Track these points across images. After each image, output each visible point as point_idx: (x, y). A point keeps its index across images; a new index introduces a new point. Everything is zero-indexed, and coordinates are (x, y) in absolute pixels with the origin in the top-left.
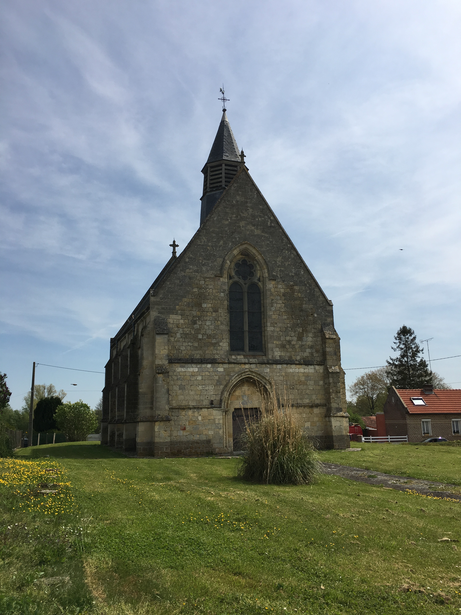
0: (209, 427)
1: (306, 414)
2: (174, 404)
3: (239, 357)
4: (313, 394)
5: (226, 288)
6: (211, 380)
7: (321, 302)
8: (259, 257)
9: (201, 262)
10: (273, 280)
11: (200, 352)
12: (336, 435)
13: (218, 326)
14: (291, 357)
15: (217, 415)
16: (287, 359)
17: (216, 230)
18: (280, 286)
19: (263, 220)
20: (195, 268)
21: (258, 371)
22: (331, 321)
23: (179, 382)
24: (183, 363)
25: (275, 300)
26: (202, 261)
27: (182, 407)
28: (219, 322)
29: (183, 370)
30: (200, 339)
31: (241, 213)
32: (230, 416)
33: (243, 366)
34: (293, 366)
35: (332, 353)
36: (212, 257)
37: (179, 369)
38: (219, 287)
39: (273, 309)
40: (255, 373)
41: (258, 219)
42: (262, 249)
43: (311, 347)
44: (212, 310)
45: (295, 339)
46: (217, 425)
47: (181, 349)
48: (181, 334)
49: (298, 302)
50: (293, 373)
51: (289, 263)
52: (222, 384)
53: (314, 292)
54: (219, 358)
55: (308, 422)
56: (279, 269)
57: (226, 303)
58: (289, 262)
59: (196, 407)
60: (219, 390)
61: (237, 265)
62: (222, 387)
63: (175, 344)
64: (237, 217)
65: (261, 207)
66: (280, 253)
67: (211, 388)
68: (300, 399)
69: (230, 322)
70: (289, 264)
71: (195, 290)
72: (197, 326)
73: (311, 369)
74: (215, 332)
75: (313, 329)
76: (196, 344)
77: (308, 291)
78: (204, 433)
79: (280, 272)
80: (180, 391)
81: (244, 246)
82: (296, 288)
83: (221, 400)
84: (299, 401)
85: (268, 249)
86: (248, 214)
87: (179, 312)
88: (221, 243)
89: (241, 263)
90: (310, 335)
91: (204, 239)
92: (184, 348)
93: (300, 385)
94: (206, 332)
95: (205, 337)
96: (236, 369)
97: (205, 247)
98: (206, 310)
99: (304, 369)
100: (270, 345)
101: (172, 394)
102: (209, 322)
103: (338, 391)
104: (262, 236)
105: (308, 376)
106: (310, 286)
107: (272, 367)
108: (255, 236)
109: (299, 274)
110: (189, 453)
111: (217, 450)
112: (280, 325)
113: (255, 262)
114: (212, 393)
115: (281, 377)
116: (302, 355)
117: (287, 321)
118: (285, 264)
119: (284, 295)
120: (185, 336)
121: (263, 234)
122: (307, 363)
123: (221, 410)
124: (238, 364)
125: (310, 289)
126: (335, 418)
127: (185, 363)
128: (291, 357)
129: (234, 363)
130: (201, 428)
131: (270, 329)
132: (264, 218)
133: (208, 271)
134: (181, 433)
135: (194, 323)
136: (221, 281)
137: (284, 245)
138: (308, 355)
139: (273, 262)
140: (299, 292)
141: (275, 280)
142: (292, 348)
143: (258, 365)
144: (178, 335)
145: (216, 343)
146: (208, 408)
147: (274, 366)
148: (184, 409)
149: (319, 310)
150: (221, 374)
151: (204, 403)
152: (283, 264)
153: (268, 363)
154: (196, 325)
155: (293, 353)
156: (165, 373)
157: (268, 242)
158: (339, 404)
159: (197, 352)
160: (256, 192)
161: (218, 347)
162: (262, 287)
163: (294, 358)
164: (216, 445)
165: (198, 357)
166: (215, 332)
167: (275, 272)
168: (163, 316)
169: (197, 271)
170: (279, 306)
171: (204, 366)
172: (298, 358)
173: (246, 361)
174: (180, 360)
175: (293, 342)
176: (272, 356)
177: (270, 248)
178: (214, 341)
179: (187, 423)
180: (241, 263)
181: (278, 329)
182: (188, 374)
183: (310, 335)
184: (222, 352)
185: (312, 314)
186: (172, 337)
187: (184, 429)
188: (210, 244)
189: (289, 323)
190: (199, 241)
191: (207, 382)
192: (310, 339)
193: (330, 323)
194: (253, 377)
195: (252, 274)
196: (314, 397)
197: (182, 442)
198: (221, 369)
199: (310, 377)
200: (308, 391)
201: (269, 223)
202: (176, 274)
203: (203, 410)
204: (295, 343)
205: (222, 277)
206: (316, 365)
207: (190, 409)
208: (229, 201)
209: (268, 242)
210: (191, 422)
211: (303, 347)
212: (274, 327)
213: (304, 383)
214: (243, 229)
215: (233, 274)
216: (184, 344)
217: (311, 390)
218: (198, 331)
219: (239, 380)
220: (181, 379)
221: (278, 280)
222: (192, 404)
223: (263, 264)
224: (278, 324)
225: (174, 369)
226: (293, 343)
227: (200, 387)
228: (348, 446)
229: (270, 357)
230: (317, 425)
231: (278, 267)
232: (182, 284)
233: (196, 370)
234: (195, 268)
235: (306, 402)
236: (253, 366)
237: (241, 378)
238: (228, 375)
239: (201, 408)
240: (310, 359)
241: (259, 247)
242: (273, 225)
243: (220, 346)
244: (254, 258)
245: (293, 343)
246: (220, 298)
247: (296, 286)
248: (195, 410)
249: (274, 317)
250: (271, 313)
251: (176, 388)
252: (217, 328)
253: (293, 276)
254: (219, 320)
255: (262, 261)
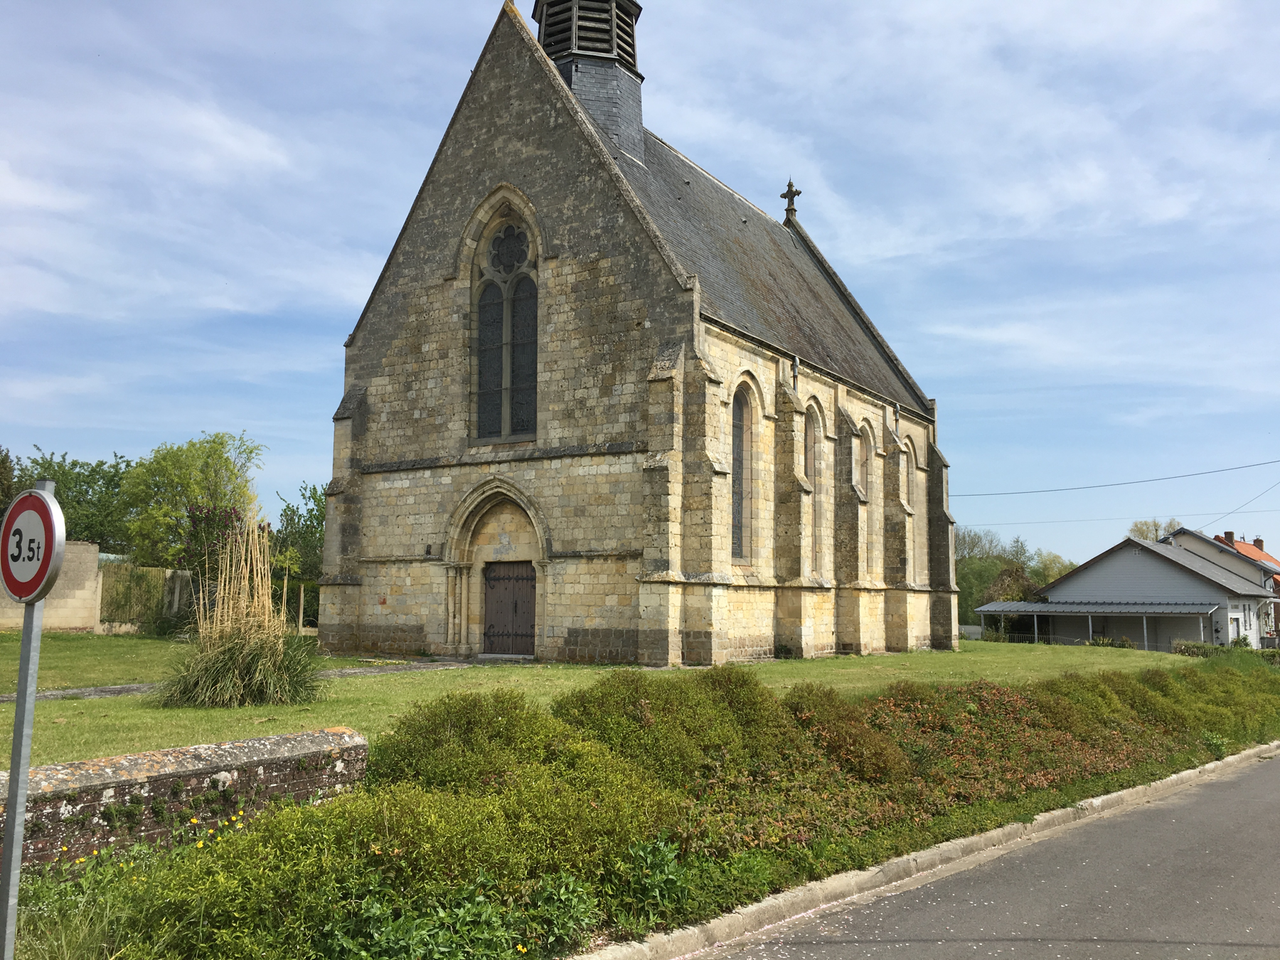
0: (421, 600)
1: (608, 575)
2: (371, 553)
3: (483, 450)
4: (627, 527)
5: (464, 301)
6: (429, 503)
7: (663, 287)
8: (527, 212)
9: (422, 256)
10: (552, 258)
11: (415, 447)
12: (645, 628)
13: (447, 387)
14: (583, 439)
15: (436, 576)
16: (576, 444)
17: (450, 176)
18: (567, 270)
19: (539, 117)
20: (413, 272)
21: (512, 479)
22: (687, 331)
23: (380, 511)
24: (385, 472)
25: (555, 307)
26: (425, 254)
27: (379, 559)
28: (449, 379)
29: (387, 485)
30: (416, 421)
31: (497, 119)
32: (477, 579)
33: (485, 469)
34: (586, 460)
35: (660, 419)
36: (441, 240)
37: (381, 485)
38: (450, 301)
39: (550, 328)
40: (508, 484)
41: (531, 118)
42: (533, 190)
43: (631, 409)
44: (436, 355)
45: (596, 392)
46: (435, 595)
47: (387, 444)
48: (388, 413)
49: (605, 300)
50: (584, 476)
51: (592, 205)
52: (444, 511)
53: (646, 264)
54: (446, 455)
55: (612, 594)
56: (568, 227)
57: (462, 334)
58: (589, 204)
59: (401, 558)
60: (441, 523)
61: (497, 242)
62: (446, 516)
63: (378, 436)
64: (489, 131)
65: (537, 87)
66: (572, 188)
67: (429, 519)
68: (595, 539)
69: (480, 373)
70: (591, 209)
71: (413, 318)
72: (412, 394)
73: (626, 463)
74: (441, 401)
75: (637, 362)
76: (409, 432)
77: (632, 266)
78: (414, 612)
79: (569, 236)
80: (379, 529)
81: (499, 196)
82: (604, 264)
83: (443, 545)
84: (594, 545)
85: (546, 184)
86: (511, 115)
87: (387, 369)
88: (458, 202)
89: (502, 235)
90: (631, 377)
91: (429, 204)
92: (392, 443)
93: (598, 505)
94: (426, 404)
95: (424, 415)
96: (474, 477)
97: (430, 222)
98: (427, 358)
99: (610, 465)
100: (541, 416)
101: (368, 534)
102: (434, 381)
103: (663, 517)
104: (537, 158)
105: (617, 483)
106: (639, 249)
107: (540, 467)
108: (523, 163)
109: (612, 227)
110: (388, 649)
111: (433, 647)
112: (563, 364)
113: (524, 226)
114: (430, 530)
115: (557, 488)
116: (610, 430)
117: (580, 353)
118: (581, 212)
119: (575, 289)
120: (394, 414)
121: (539, 153)
122: (614, 451)
123: (443, 565)
124: (477, 464)
125: (638, 260)
126: (648, 586)
127: (391, 472)
128: (583, 439)
129: (471, 464)
130: (409, 602)
131: (542, 377)
132: (543, 111)
133: (433, 272)
134: (379, 609)
135: (408, 387)
136: (455, 287)
137: (583, 163)
138: (624, 431)
139: (555, 215)
140: (611, 272)
141: (556, 257)
142: (586, 416)
143: (513, 464)
144: (384, 417)
145: (441, 425)
146: (422, 561)
147: (546, 464)
148: (384, 563)
149: (658, 310)
150: (446, 489)
151: (417, 552)
152: (577, 213)
153: (531, 459)
154: (411, 392)
155: (590, 428)
156: (339, 493)
157: (547, 168)
158: (664, 550)
159: (411, 447)
160: (529, 53)
161: (446, 434)
162: (535, 280)
163: (590, 440)
164: (434, 639)
165: (411, 457)
166: (441, 401)
167: (557, 239)
168: (361, 383)
169: (415, 279)
170: (563, 317)
171: (419, 474)
172: (600, 439)
173: (490, 457)
174: (381, 466)
175: (591, 401)
176: (545, 440)
177: (550, 182)
178: (439, 421)
179: (389, 590)
180: (502, 235)
181: (558, 376)
182: (393, 493)
183: (631, 377)
184: (451, 443)
185: (639, 324)
186: (374, 421)
187: (384, 602)
188: (439, 212)
189: (583, 355)
190: (421, 213)
191: (423, 507)
192: (629, 388)
193: (681, 339)
194: (504, 491)
195: (523, 255)
196: (629, 534)
197: (378, 628)
198: (446, 480)
199: (621, 486)
200: (615, 519)
201: (552, 120)
202: (384, 293)
203: (414, 565)
204: (594, 404)
205: (455, 279)
206: (637, 452)
207: (394, 562)
208: (475, 100)
209: (547, 168)
210: (395, 588)
211: (612, 410)
212: (551, 371)
213: (607, 501)
214: (500, 155)
215: (485, 264)
216: (393, 433)
217: (621, 516)
218: (413, 404)
219: (479, 500)
220: (383, 504)
221: (565, 256)
222: (398, 552)
223: (533, 226)
224: (559, 363)
225: (373, 485)
226: (590, 403)
227: (412, 517)
228: (705, 660)
229: (540, 443)
230: (633, 604)
231: (566, 223)
232: (392, 312)
233: (406, 484)
234: (413, 272)
235: (609, 547)
236: (504, 467)
237: (484, 496)
238: (459, 491)
239: (411, 562)
240: (626, 439)
241: (528, 188)
242: (560, 121)
243: (448, 429)
244: (521, 219)
245: (590, 403)
246: (451, 325)
247: (605, 261)
248: (402, 566)
249: (551, 347)
250: (545, 341)
251: (375, 522)
252: (445, 392)
253: (598, 237)
254: (448, 375)
255: (531, 220)
